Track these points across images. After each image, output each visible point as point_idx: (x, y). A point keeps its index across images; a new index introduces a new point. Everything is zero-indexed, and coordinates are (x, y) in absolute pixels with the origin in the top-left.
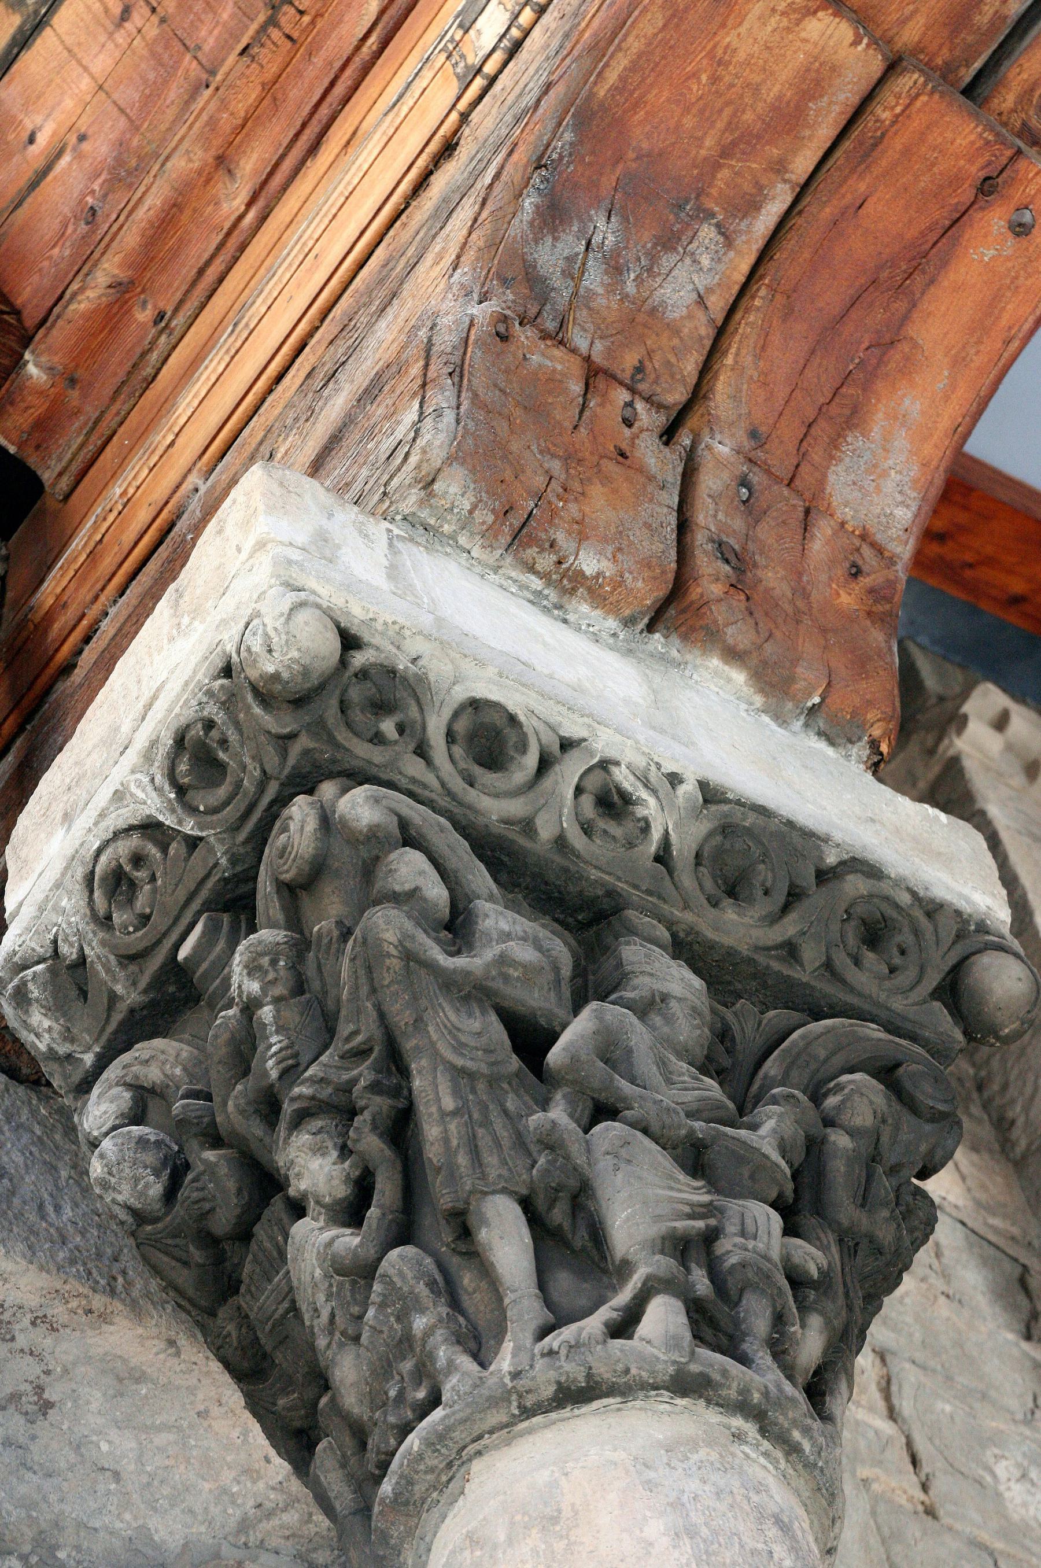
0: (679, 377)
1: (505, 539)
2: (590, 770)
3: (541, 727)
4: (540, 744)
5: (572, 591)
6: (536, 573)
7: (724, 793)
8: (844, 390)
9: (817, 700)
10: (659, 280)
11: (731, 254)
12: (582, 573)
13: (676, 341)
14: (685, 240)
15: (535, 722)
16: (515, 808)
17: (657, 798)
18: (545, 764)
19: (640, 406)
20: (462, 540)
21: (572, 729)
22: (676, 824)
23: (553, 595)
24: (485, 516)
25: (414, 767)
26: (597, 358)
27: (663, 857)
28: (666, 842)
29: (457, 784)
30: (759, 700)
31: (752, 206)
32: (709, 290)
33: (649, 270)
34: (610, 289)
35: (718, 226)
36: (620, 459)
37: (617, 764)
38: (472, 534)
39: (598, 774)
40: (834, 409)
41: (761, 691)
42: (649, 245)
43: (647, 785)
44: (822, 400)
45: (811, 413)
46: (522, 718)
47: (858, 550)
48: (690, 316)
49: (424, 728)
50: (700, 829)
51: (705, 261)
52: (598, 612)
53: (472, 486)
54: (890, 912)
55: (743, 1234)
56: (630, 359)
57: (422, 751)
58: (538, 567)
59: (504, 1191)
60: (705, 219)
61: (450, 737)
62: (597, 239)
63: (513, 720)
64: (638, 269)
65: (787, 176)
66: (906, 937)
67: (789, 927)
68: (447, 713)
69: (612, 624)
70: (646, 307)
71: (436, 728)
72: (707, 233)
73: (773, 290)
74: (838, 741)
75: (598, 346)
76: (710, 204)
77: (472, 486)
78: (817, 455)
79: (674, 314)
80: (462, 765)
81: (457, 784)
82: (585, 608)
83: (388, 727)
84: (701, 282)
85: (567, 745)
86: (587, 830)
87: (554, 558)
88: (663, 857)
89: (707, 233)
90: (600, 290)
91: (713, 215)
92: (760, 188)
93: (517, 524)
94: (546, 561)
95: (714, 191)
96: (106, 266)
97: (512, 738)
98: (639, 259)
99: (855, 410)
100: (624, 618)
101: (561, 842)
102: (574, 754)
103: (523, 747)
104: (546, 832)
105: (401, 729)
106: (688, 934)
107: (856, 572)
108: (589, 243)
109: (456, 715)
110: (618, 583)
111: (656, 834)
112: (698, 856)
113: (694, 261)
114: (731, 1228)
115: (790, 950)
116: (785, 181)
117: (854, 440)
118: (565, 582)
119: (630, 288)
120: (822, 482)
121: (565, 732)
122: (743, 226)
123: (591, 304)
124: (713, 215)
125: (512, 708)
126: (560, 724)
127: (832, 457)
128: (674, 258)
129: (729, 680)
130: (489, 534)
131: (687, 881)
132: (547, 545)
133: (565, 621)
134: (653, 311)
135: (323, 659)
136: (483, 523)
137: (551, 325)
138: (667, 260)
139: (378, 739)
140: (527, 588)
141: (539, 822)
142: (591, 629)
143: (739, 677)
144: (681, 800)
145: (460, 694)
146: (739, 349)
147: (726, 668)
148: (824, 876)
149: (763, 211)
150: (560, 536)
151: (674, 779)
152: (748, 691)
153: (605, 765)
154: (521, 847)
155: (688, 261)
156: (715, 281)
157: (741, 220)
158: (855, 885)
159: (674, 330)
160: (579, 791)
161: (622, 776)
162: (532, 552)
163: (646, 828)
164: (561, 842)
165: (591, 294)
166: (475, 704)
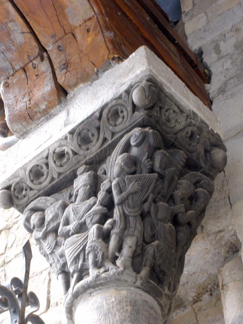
0: (34, 48)
1: (31, 121)
3: (41, 161)
4: (43, 163)
5: (48, 112)
6: (41, 118)
7: (74, 129)
8: (56, 7)
9: (96, 69)
10: (15, 41)
11: (16, 21)
12: (44, 109)
13: (28, 44)
14: (10, 30)
15: (40, 161)
18: (47, 165)
19: (34, 62)
20: (28, 128)
21: (45, 155)
22: (72, 146)
23: (48, 116)
24: (24, 124)
25: (31, 193)
26: (22, 65)
27: (75, 153)
28: (73, 151)
29: (39, 187)
30: (89, 83)
31: (8, 12)
32: (22, 30)
33: (13, 42)
34: (12, 53)
35: (10, 22)
36: (38, 77)
37: (56, 149)
38: (28, 126)
40: (58, 12)
41: (87, 82)
42: (8, 39)
44: (55, 14)
45: (56, 18)
47: (86, 26)
48: (25, 38)
49: (28, 186)
51: (16, 28)
52: (55, 109)
53: (17, 123)
54: (115, 108)
56: (26, 57)
57: (31, 189)
58: (39, 117)
60: (7, 24)
61: (32, 181)
62: (2, 50)
63: (38, 165)
65: (4, 2)
66: (120, 108)
69: (58, 107)
70: (19, 46)
71: (29, 183)
72: (10, 25)
73: (27, 15)
74: (107, 68)
75: (20, 63)
76: (4, 22)
77: (17, 123)
78: (65, 23)
79: (23, 41)
80: (38, 183)
81: (39, 187)
82: (52, 111)
84: (19, 31)
85: (47, 158)
86: (61, 166)
87: (38, 113)
88: (75, 153)
89: (10, 25)
90: (11, 55)
91: (7, 22)
92: (4, 9)
93: (29, 117)
94: (39, 115)
95: (2, 20)
96: (48, 73)
97: (39, 168)
98: (10, 43)
99: (61, 7)
100: (58, 104)
101: (60, 174)
103: (42, 168)
104: (56, 176)
106: (90, 160)
107: (88, 31)
108: (3, 53)
110: (49, 102)
111: (70, 152)
113: (15, 30)
115: (105, 140)
116: (5, 3)
117: (67, 10)
118: (45, 113)
119: (14, 48)
120: (70, 25)
121: (45, 156)
122: (11, 16)
123: (13, 59)
124: (7, 22)
126: (43, 156)
127: (67, 19)
128: (12, 35)
129: (81, 88)
130: (28, 124)
132: (35, 113)
133: (55, 115)
134: (20, 46)
135: (4, 200)
136: (26, 124)
137: (11, 72)
138: (12, 37)
140: (44, 120)
141: (54, 176)
142: (58, 111)
143: (82, 85)
145: (27, 173)
146: (36, 29)
147: (78, 87)
148: (100, 118)
149: (10, 10)
150: (35, 110)
151: (66, 138)
152: (86, 84)
154: (55, 183)
155: (14, 32)
156: (21, 28)
157: (10, 16)
159: (26, 43)
160: (55, 162)
162: (36, 117)
163: (68, 153)
164: (60, 174)
165: (11, 58)
166: (31, 171)
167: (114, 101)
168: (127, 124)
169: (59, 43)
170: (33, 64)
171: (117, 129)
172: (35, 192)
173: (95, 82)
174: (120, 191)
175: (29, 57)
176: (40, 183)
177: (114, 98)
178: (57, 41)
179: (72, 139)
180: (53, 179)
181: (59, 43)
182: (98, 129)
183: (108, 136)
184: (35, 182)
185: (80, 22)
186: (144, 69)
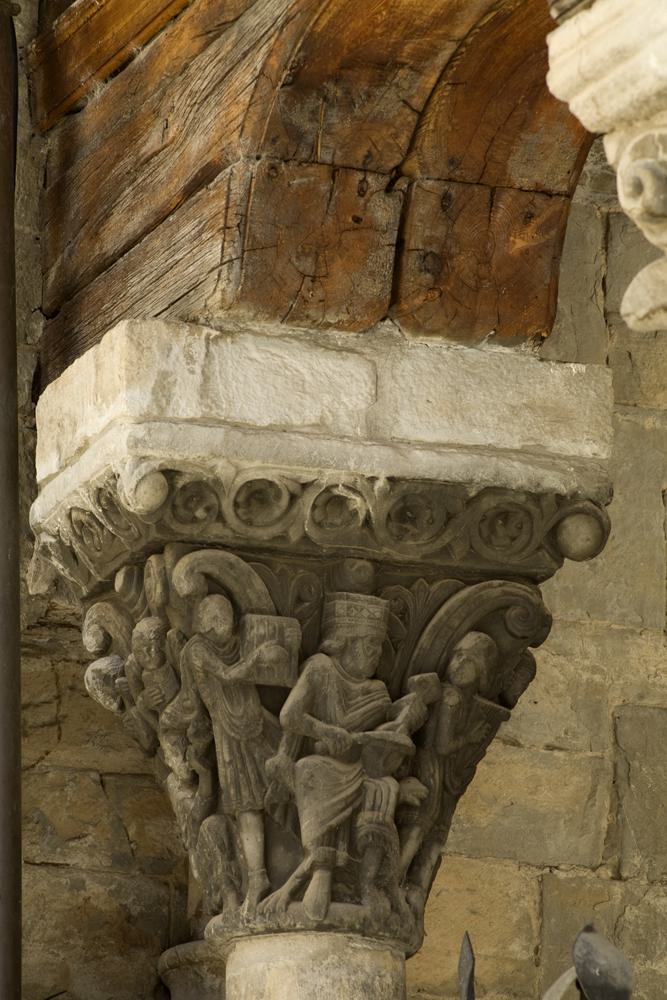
2: (320, 494)
3: (288, 483)
4: (289, 491)
16: (276, 530)
17: (362, 496)
18: (293, 498)
22: (374, 507)
26: (338, 161)
35: (411, 68)
39: (325, 497)
43: (354, 491)
46: (277, 482)
47: (531, 202)
49: (220, 506)
50: (387, 506)
55: (373, 809)
56: (361, 153)
57: (220, 517)
59: (250, 810)
61: (236, 505)
63: (271, 484)
64: (361, 102)
67: (446, 538)
68: (233, 495)
80: (244, 518)
83: (200, 513)
85: (305, 486)
88: (367, 521)
91: (407, 64)
102: (310, 489)
103: (278, 496)
105: (208, 510)
109: (238, 493)
111: (362, 516)
112: (389, 515)
114: (368, 805)
115: (446, 551)
120: (504, 172)
121: (302, 482)
125: (270, 479)
128: (383, 89)
131: (382, 534)
137: (304, 155)
139: (195, 520)
141: (291, 533)
144: (376, 493)
145: (240, 481)
150: (312, 313)
153: (328, 489)
158: (489, 503)
160: (314, 507)
161: (340, 491)
164: (305, 538)
166: (250, 483)
167: (523, 498)
168: (515, 561)
169: (454, 190)
170: (364, 180)
171: (488, 553)
172: (227, 532)
173: (462, 347)
174: (456, 734)
175: (369, 155)
176: (249, 523)
177: (526, 489)
178: (450, 180)
179: (385, 495)
180: (283, 537)
181: (454, 190)
182: (450, 517)
183: (459, 551)
184: (240, 511)
185: (526, 183)
186: (604, 456)
